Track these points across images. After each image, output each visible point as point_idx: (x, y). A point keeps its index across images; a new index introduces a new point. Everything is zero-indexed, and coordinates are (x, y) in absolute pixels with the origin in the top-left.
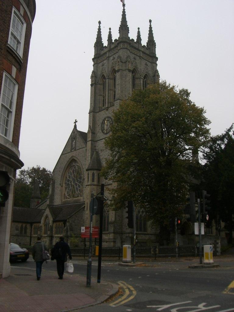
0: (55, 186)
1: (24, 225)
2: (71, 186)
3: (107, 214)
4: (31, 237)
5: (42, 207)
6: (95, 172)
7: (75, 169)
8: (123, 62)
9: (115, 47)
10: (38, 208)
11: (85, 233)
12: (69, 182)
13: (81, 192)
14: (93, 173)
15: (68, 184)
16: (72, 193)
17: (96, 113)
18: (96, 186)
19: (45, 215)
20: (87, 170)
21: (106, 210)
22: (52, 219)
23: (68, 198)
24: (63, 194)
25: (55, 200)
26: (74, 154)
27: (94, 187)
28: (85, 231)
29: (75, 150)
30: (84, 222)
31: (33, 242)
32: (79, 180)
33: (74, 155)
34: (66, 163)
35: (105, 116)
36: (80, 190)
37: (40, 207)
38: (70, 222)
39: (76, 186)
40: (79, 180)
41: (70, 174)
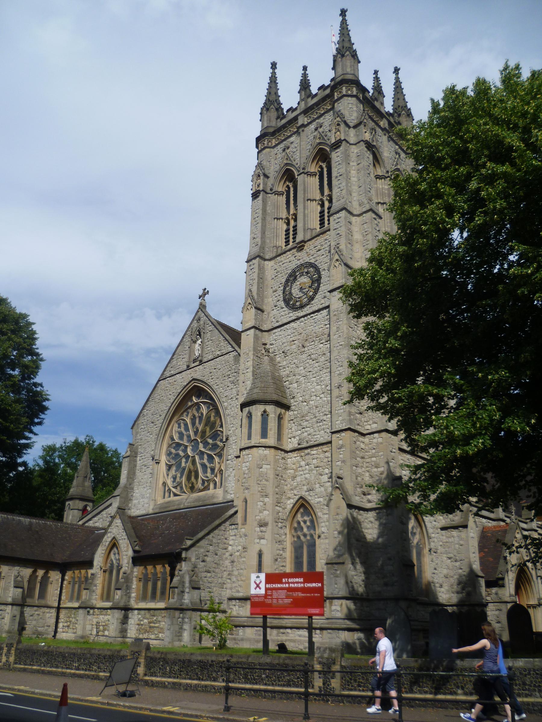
0: (138, 462)
1: (40, 573)
2: (184, 460)
3: (308, 538)
4: (59, 609)
5: (98, 522)
6: (270, 408)
7: (197, 415)
8: (349, 127)
9: (317, 104)
10: (86, 524)
11: (266, 596)
12: (178, 450)
13: (216, 476)
14: (265, 411)
15: (177, 455)
16: (189, 478)
17: (266, 262)
18: (273, 450)
19: (107, 539)
20: (243, 406)
21: (302, 523)
22: (130, 553)
23: (175, 495)
24: (161, 482)
25: (135, 502)
26: (198, 373)
27: (267, 452)
28: (267, 589)
29: (201, 363)
30: (233, 562)
31: (66, 624)
32: (210, 441)
33: (197, 376)
34: (172, 398)
35: (293, 265)
36: (213, 470)
37: (91, 522)
38: (193, 559)
39: (202, 458)
40: (210, 441)
41: (182, 429)
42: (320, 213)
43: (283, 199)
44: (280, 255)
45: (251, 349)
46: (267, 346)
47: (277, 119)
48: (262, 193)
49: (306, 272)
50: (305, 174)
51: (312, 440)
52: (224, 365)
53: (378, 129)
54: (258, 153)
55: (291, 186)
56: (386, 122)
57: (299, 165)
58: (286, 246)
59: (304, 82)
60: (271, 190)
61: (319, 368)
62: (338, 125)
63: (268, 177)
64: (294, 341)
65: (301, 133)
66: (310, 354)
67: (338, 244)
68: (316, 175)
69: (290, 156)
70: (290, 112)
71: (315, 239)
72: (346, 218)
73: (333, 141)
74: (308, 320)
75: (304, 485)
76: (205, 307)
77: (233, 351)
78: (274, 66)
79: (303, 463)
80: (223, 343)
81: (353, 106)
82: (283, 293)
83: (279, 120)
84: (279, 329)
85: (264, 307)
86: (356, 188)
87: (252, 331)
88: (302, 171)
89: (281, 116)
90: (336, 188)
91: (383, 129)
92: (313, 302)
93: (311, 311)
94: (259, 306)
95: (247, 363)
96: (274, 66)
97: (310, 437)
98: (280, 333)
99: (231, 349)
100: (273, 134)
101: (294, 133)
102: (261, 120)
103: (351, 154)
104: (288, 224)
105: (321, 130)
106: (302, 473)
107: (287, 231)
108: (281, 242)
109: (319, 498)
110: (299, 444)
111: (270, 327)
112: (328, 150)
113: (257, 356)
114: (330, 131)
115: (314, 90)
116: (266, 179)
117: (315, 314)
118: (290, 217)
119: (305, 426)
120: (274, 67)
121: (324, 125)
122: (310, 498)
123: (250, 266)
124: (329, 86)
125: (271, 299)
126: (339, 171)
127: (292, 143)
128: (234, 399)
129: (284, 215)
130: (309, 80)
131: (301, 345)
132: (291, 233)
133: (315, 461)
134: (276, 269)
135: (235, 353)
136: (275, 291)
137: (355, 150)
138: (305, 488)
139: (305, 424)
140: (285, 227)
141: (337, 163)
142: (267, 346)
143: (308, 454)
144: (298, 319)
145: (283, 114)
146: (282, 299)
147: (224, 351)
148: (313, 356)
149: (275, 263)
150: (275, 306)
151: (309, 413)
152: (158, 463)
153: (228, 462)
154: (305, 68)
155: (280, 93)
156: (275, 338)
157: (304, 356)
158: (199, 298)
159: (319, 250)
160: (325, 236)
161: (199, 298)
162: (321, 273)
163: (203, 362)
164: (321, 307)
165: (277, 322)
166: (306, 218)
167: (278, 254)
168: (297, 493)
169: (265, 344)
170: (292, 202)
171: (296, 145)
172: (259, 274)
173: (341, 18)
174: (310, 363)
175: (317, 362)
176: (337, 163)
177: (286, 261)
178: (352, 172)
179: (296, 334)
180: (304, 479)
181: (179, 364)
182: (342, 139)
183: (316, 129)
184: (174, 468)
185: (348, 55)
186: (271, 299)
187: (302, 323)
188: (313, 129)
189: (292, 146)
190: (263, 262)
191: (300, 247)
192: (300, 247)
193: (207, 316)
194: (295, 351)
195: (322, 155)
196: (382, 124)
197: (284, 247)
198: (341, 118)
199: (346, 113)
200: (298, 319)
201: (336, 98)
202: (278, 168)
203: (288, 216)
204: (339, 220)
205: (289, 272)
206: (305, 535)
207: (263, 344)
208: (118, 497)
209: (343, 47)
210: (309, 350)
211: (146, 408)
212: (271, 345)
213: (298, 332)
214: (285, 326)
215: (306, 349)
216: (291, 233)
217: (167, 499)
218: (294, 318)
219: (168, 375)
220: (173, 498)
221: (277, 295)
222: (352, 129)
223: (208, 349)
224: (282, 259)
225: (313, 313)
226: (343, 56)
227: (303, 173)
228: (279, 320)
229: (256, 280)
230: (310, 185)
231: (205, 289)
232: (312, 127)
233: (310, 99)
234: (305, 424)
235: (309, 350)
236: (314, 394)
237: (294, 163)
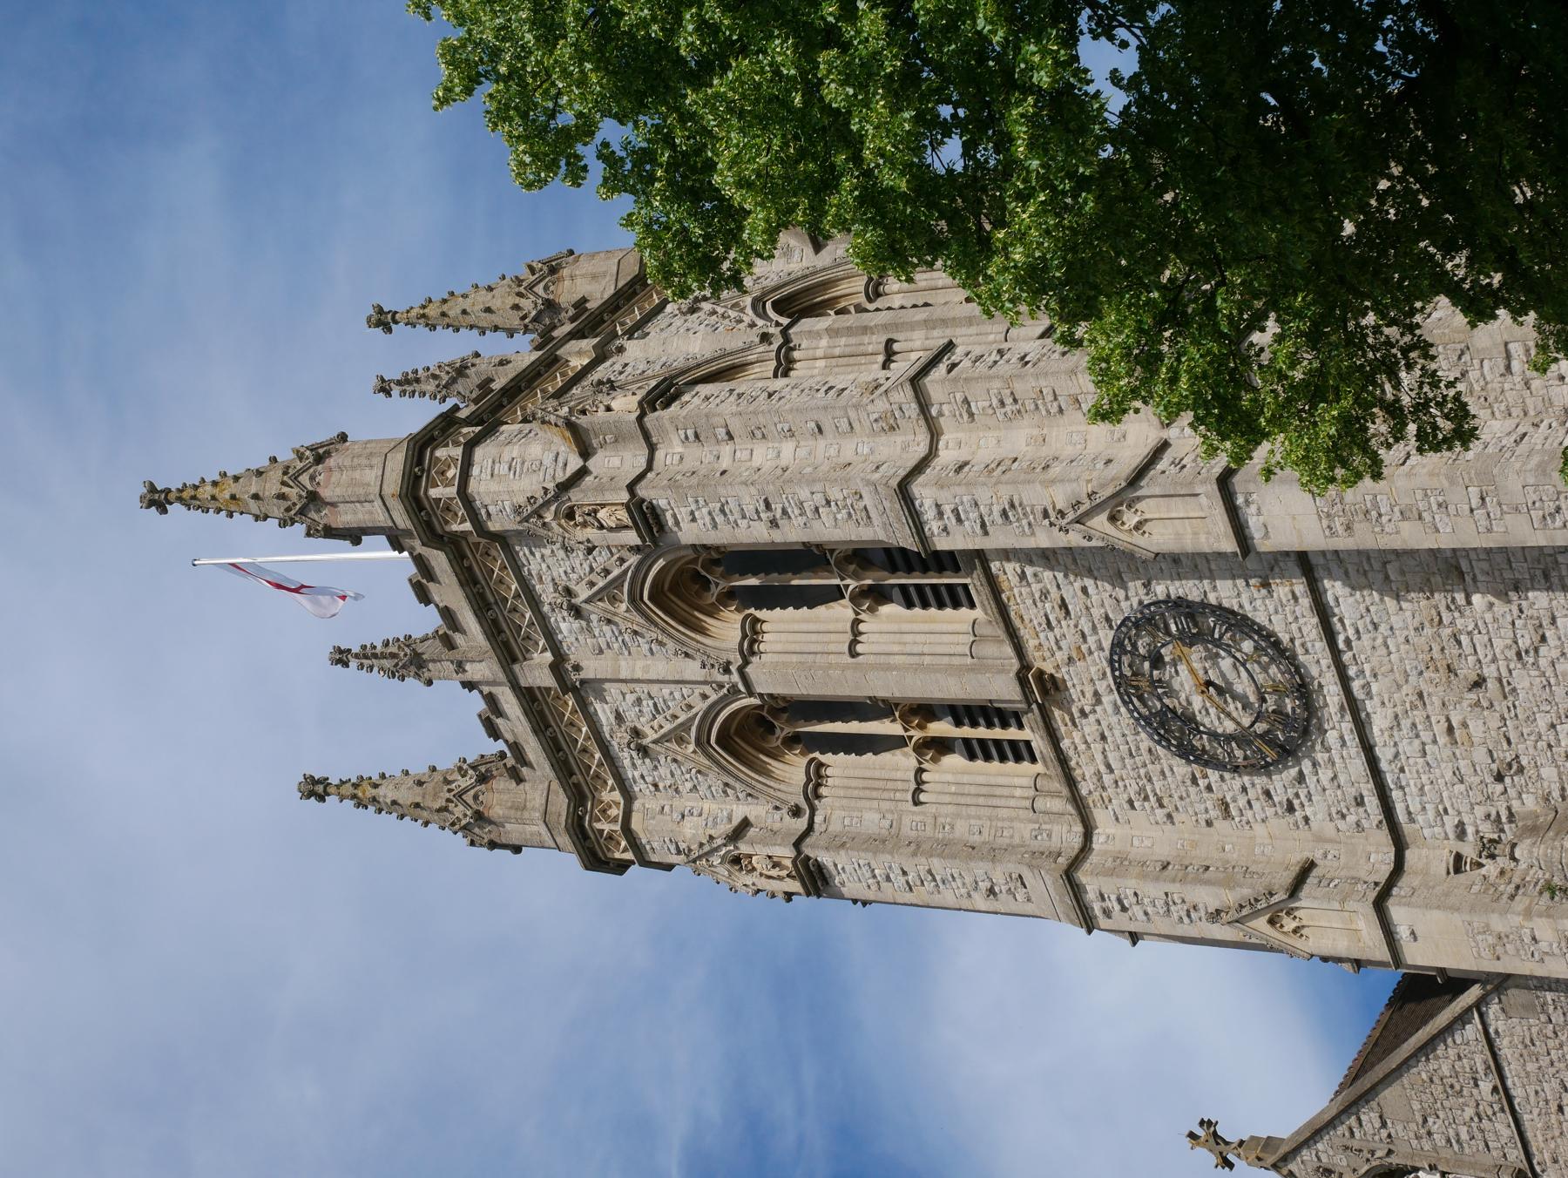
8: (582, 472)
9: (482, 605)
17: (1098, 842)
42: (909, 605)
43: (838, 764)
44: (1071, 782)
45: (1478, 921)
46: (1469, 850)
47: (519, 780)
48: (807, 850)
49: (1154, 666)
50: (746, 663)
52: (1544, 1062)
53: (601, 373)
54: (646, 863)
55: (788, 730)
56: (574, 345)
57: (707, 690)
58: (1033, 760)
59: (387, 663)
60: (796, 812)
62: (570, 515)
63: (746, 823)
64: (1450, 730)
65: (583, 675)
66: (1511, 654)
67: (1046, 514)
68: (756, 620)
69: (668, 727)
70: (499, 721)
71: (1017, 622)
72: (940, 485)
73: (632, 538)
74: (1364, 655)
76: (1270, 1143)
77: (1481, 1016)
78: (315, 789)
80: (1443, 1061)
81: (506, 457)
82: (1236, 769)
83: (525, 771)
84: (1396, 795)
85: (1296, 858)
86: (821, 443)
87: (1398, 913)
88: (736, 677)
89: (510, 761)
90: (816, 524)
91: (600, 357)
92: (1285, 638)
93: (1320, 647)
94: (1287, 878)
95: (1543, 946)
96: (315, 789)
98: (1412, 789)
99: (1472, 1030)
100: (579, 796)
101: (583, 705)
102: (517, 849)
103: (689, 464)
104: (942, 746)
105: (583, 593)
107: (974, 750)
108: (1018, 774)
111: (1384, 836)
112: (661, 563)
113: (1512, 897)
114: (590, 551)
115: (426, 621)
116: (752, 832)
117: (1338, 627)
118: (917, 734)
120: (320, 789)
121: (563, 581)
123: (1107, 913)
124: (419, 561)
125: (1259, 829)
126: (749, 510)
127: (619, 717)
129: (904, 761)
130: (386, 644)
131: (1473, 696)
132: (982, 732)
134: (1131, 802)
135: (1493, 1010)
136: (1225, 806)
137: (672, 451)
140: (954, 761)
141: (719, 519)
142: (1469, 850)
144: (1353, 706)
145: (502, 755)
146: (1261, 781)
147: (1481, 1058)
148: (1524, 643)
149: (1106, 803)
150: (1291, 809)
154: (341, 657)
155: (419, 769)
156: (1431, 814)
157: (1523, 680)
158: (1231, 1165)
159: (1064, 605)
160: (1007, 572)
161: (1231, 1165)
162: (1161, 597)
163: (1524, 1166)
164: (1305, 602)
165: (1360, 801)
166: (927, 660)
167: (1065, 791)
169: (1458, 858)
170: (854, 727)
171: (630, 698)
172: (1143, 876)
173: (175, 509)
174: (1555, 653)
175: (1553, 621)
176: (719, 519)
177: (1099, 758)
178: (757, 460)
179: (1418, 716)
182: (625, 497)
183: (577, 612)
185: (312, 478)
186: (1259, 829)
187: (1375, 688)
188: (576, 624)
189: (630, 714)
190: (1094, 858)
191: (1045, 692)
192: (1044, 690)
193: (1315, 1133)
194: (1494, 722)
195: (688, 583)
196: (578, 363)
197: (1039, 767)
198: (546, 504)
199: (529, 486)
200: (1353, 706)
201: (467, 526)
202: (715, 780)
203: (909, 749)
204: (947, 509)
205: (1145, 741)
207: (1458, 870)
209: (282, 497)
210: (1494, 660)
212: (1461, 832)
213: (1414, 707)
214: (1384, 765)
215: (1489, 671)
216: (982, 732)
218: (1347, 725)
221: (1242, 802)
222: (591, 464)
223: (1464, 1136)
224: (1089, 771)
225: (1330, 635)
226: (313, 498)
227: (741, 670)
228: (1352, 792)
229: (1170, 888)
230: (800, 647)
231: (1192, 1136)
232: (566, 627)
233: (458, 638)
235: (1494, 660)
237: (700, 707)
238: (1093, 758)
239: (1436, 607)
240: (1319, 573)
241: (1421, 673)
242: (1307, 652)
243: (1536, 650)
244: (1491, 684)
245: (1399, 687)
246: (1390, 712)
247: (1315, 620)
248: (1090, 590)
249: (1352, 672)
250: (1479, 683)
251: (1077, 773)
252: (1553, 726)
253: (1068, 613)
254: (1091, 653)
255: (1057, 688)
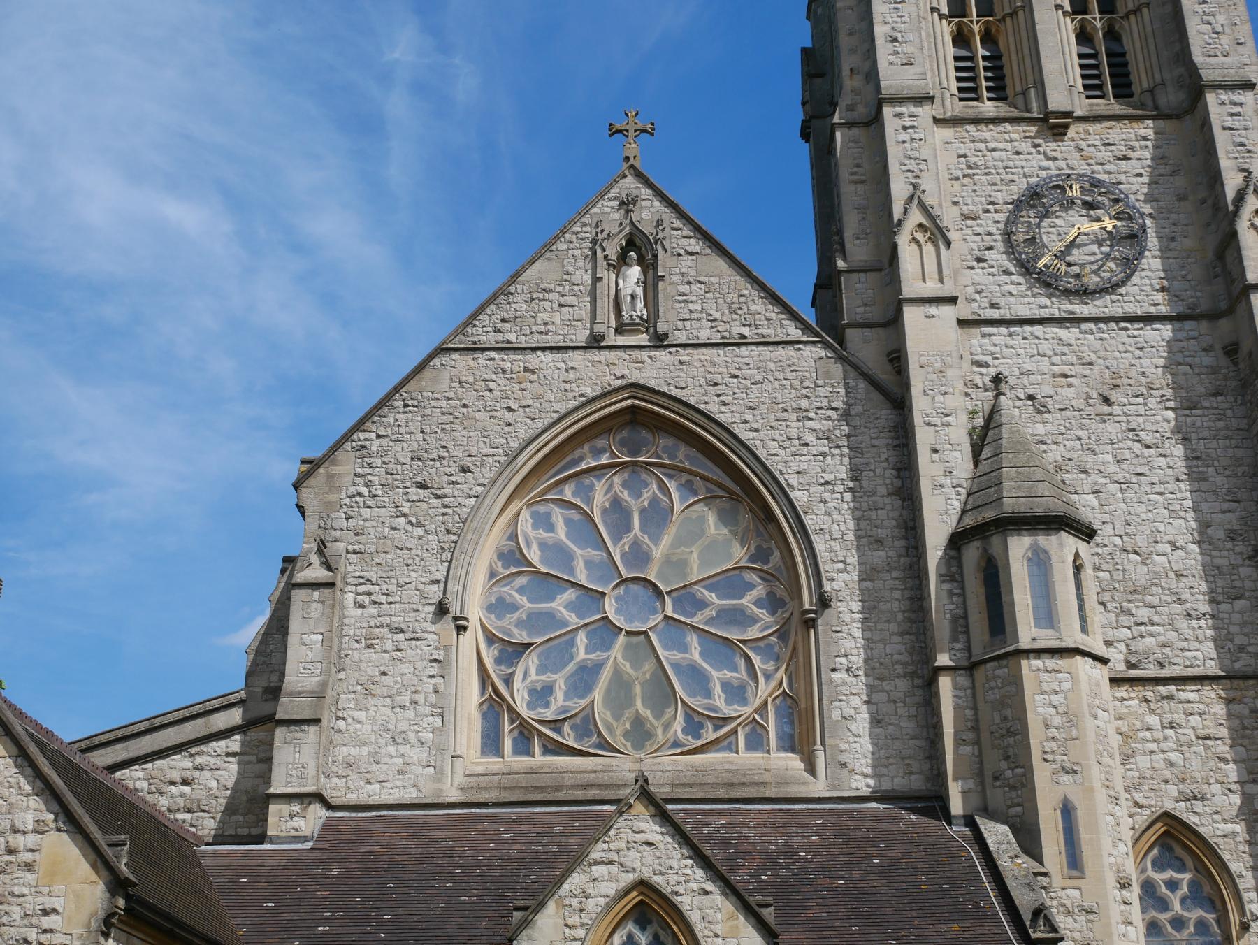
51: (1175, 661)
52: (779, 375)
61: (1170, 472)
75: (1167, 781)
79: (1153, 720)
84: (1004, 330)
90: (1197, 20)
92: (1122, 290)
93: (1117, 311)
97: (1167, 650)
106: (1153, 746)
109: (1225, 821)
110: (1131, 666)
117: (1136, 326)
119: (1145, 620)
122: (1196, 819)
128: (840, 488)
133: (1195, 720)
138: (1173, 790)
139: (1144, 614)
143: (1170, 697)
144: (1077, 320)
148: (1143, 435)
150: (979, 260)
151: (1155, 585)
152: (465, 628)
153: (835, 675)
157: (1112, 429)
168: (1145, 802)
177: (1001, 146)
180: (1162, 765)
181: (542, 317)
184: (531, 661)
206: (1178, 923)
208: (312, 730)
211: (368, 424)
213: (1079, 358)
215: (1116, 410)
217: (512, 760)
219: (490, 339)
220: (540, 759)
221: (979, 230)
234: (1144, 614)
235: (1125, 414)
236: (1167, 538)
238: (997, 141)
239: (1162, 388)
240: (1178, 325)
241: (1107, 368)
242: (1113, 302)
243: (1138, 441)
244: (1106, 409)
245: (1095, 352)
246: (1073, 342)
247: (1139, 313)
248: (1139, 179)
249: (1101, 325)
250: (1107, 401)
251: (983, 127)
252: (1079, 439)
253: (1120, 159)
254: (1089, 165)
255: (1054, 135)
